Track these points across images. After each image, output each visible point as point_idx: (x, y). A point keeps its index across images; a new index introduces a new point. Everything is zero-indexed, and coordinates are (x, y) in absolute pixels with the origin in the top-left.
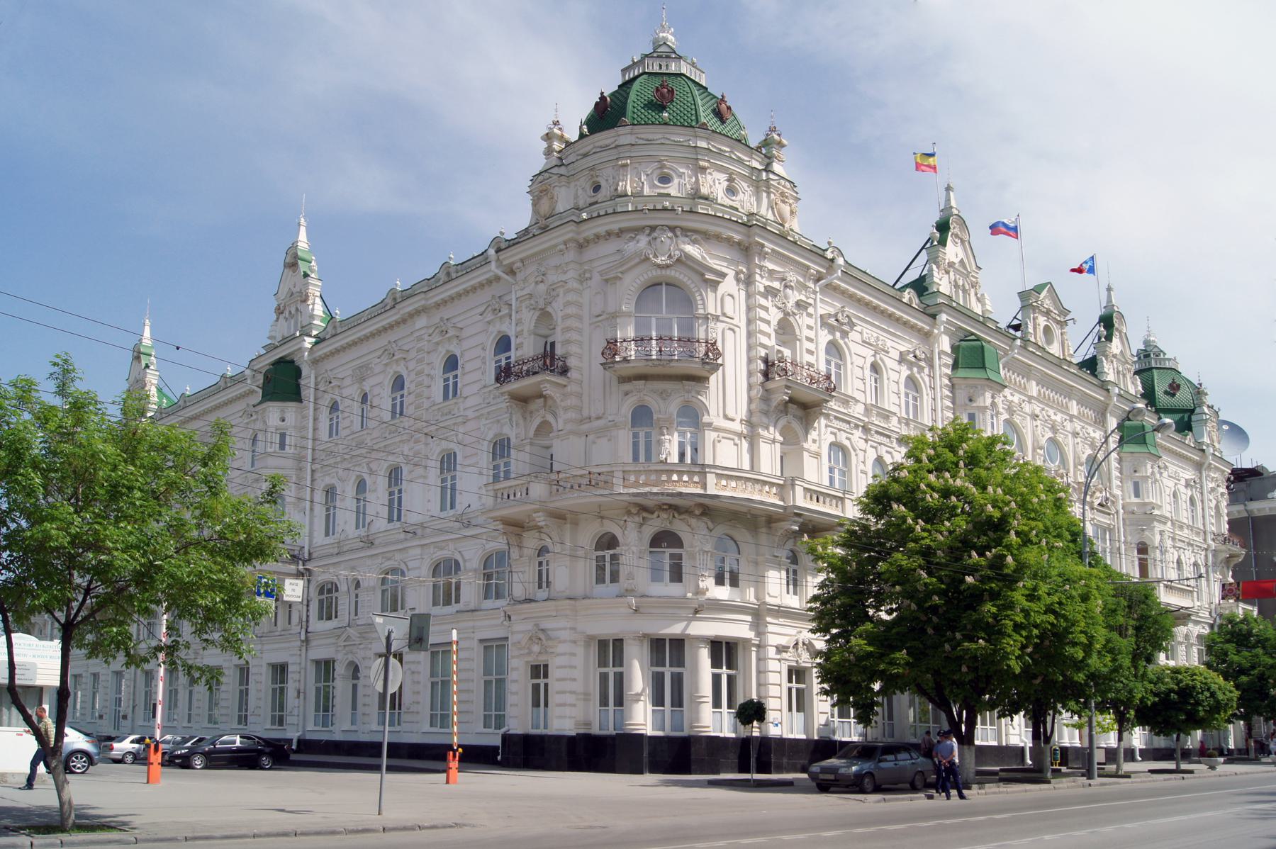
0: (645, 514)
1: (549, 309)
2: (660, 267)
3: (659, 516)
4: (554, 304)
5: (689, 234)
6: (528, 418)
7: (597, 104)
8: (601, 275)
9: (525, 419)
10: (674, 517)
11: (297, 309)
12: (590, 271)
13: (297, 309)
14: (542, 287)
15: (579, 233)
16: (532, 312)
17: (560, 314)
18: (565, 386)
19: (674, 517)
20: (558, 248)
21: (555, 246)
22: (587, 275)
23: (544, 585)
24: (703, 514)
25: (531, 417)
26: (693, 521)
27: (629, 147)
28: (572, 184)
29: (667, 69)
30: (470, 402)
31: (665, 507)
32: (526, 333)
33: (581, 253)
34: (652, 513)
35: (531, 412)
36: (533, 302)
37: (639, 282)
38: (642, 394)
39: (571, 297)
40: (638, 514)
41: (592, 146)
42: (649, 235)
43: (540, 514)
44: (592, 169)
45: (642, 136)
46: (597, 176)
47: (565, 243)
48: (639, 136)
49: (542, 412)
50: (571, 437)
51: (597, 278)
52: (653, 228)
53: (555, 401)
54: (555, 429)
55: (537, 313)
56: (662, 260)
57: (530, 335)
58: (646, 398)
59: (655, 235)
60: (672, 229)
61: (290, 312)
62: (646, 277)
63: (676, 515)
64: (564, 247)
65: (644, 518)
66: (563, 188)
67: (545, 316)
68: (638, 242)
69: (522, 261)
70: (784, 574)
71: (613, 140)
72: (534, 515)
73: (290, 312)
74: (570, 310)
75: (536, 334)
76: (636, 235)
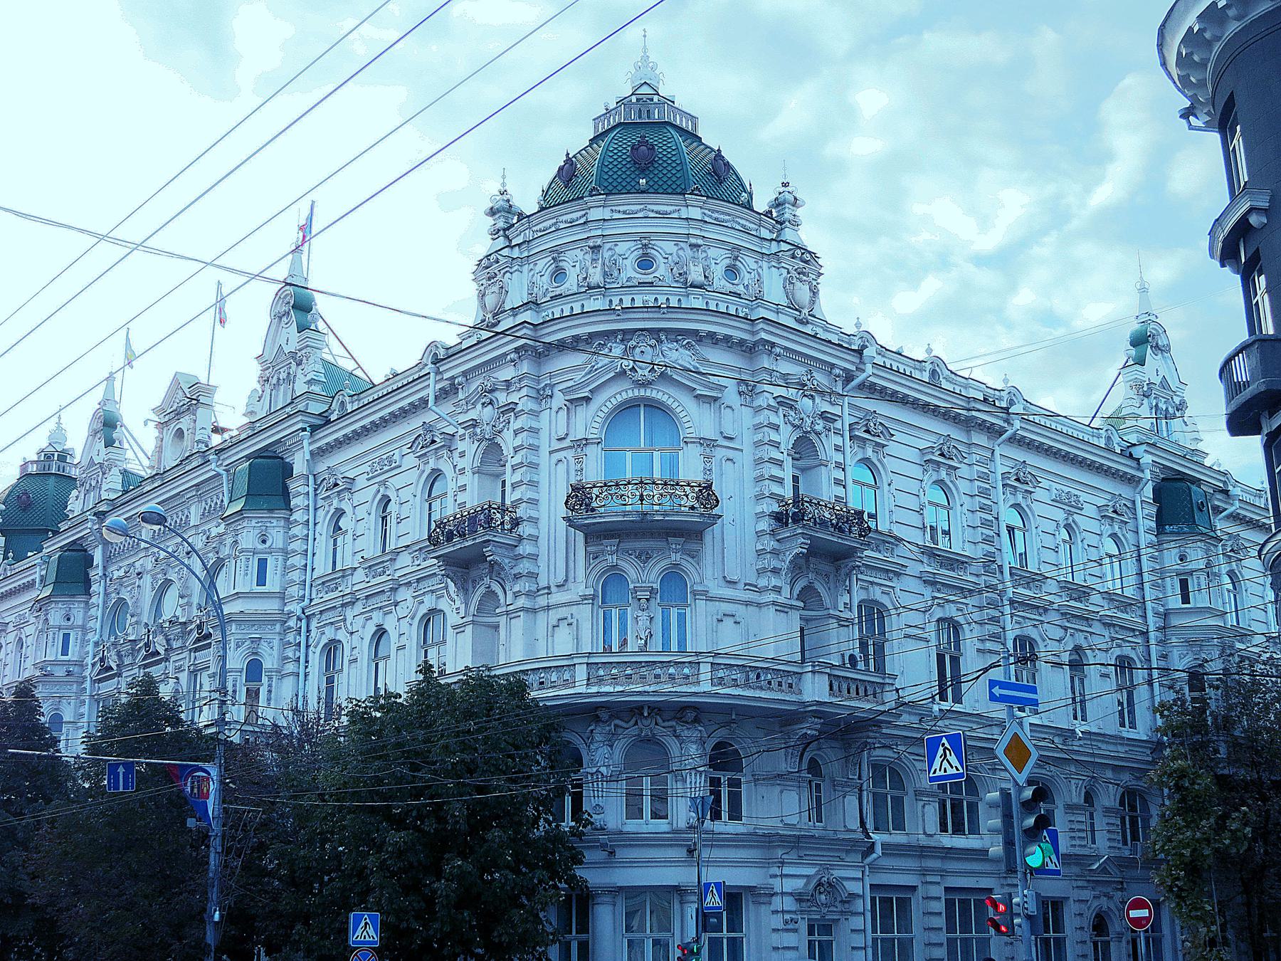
1: (499, 440)
5: (680, 338)
6: (471, 589)
7: (561, 169)
10: (656, 724)
12: (552, 386)
18: (516, 546)
21: (505, 355)
24: (697, 720)
25: (474, 588)
29: (649, 117)
33: (539, 364)
42: (622, 340)
47: (517, 350)
49: (487, 580)
50: (521, 613)
51: (559, 400)
53: (503, 569)
54: (502, 601)
59: (633, 343)
63: (660, 721)
64: (517, 355)
65: (616, 726)
67: (492, 450)
69: (464, 374)
70: (806, 794)
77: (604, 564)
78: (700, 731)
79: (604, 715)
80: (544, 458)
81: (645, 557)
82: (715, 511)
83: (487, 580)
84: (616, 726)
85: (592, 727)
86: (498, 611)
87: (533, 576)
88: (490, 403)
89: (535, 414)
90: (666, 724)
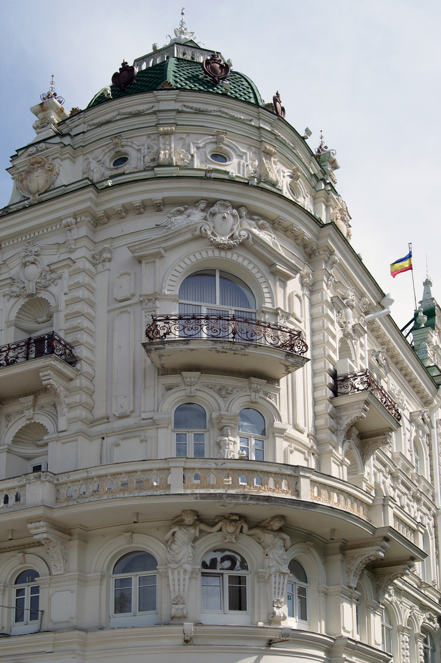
0: (203, 527)
2: (220, 247)
3: (220, 530)
4: (52, 288)
5: (256, 217)
8: (133, 252)
10: (241, 531)
14: (32, 270)
15: (97, 205)
17: (64, 298)
18: (71, 380)
19: (241, 531)
20: (64, 222)
21: (60, 220)
22: (106, 255)
27: (174, 113)
28: (80, 159)
31: (234, 517)
34: (213, 525)
35: (8, 416)
36: (14, 289)
37: (184, 266)
38: (193, 388)
39: (81, 278)
40: (193, 525)
41: (116, 113)
43: (42, 523)
44: (118, 135)
45: (191, 105)
46: (123, 146)
48: (186, 104)
52: (211, 203)
55: (22, 302)
56: (223, 239)
58: (199, 394)
60: (237, 207)
62: (199, 257)
64: (73, 221)
65: (201, 531)
66: (68, 161)
68: (189, 216)
71: (150, 105)
72: (29, 526)
74: (81, 293)
75: (17, 327)
76: (186, 209)
85: (174, 530)
88: (33, 263)
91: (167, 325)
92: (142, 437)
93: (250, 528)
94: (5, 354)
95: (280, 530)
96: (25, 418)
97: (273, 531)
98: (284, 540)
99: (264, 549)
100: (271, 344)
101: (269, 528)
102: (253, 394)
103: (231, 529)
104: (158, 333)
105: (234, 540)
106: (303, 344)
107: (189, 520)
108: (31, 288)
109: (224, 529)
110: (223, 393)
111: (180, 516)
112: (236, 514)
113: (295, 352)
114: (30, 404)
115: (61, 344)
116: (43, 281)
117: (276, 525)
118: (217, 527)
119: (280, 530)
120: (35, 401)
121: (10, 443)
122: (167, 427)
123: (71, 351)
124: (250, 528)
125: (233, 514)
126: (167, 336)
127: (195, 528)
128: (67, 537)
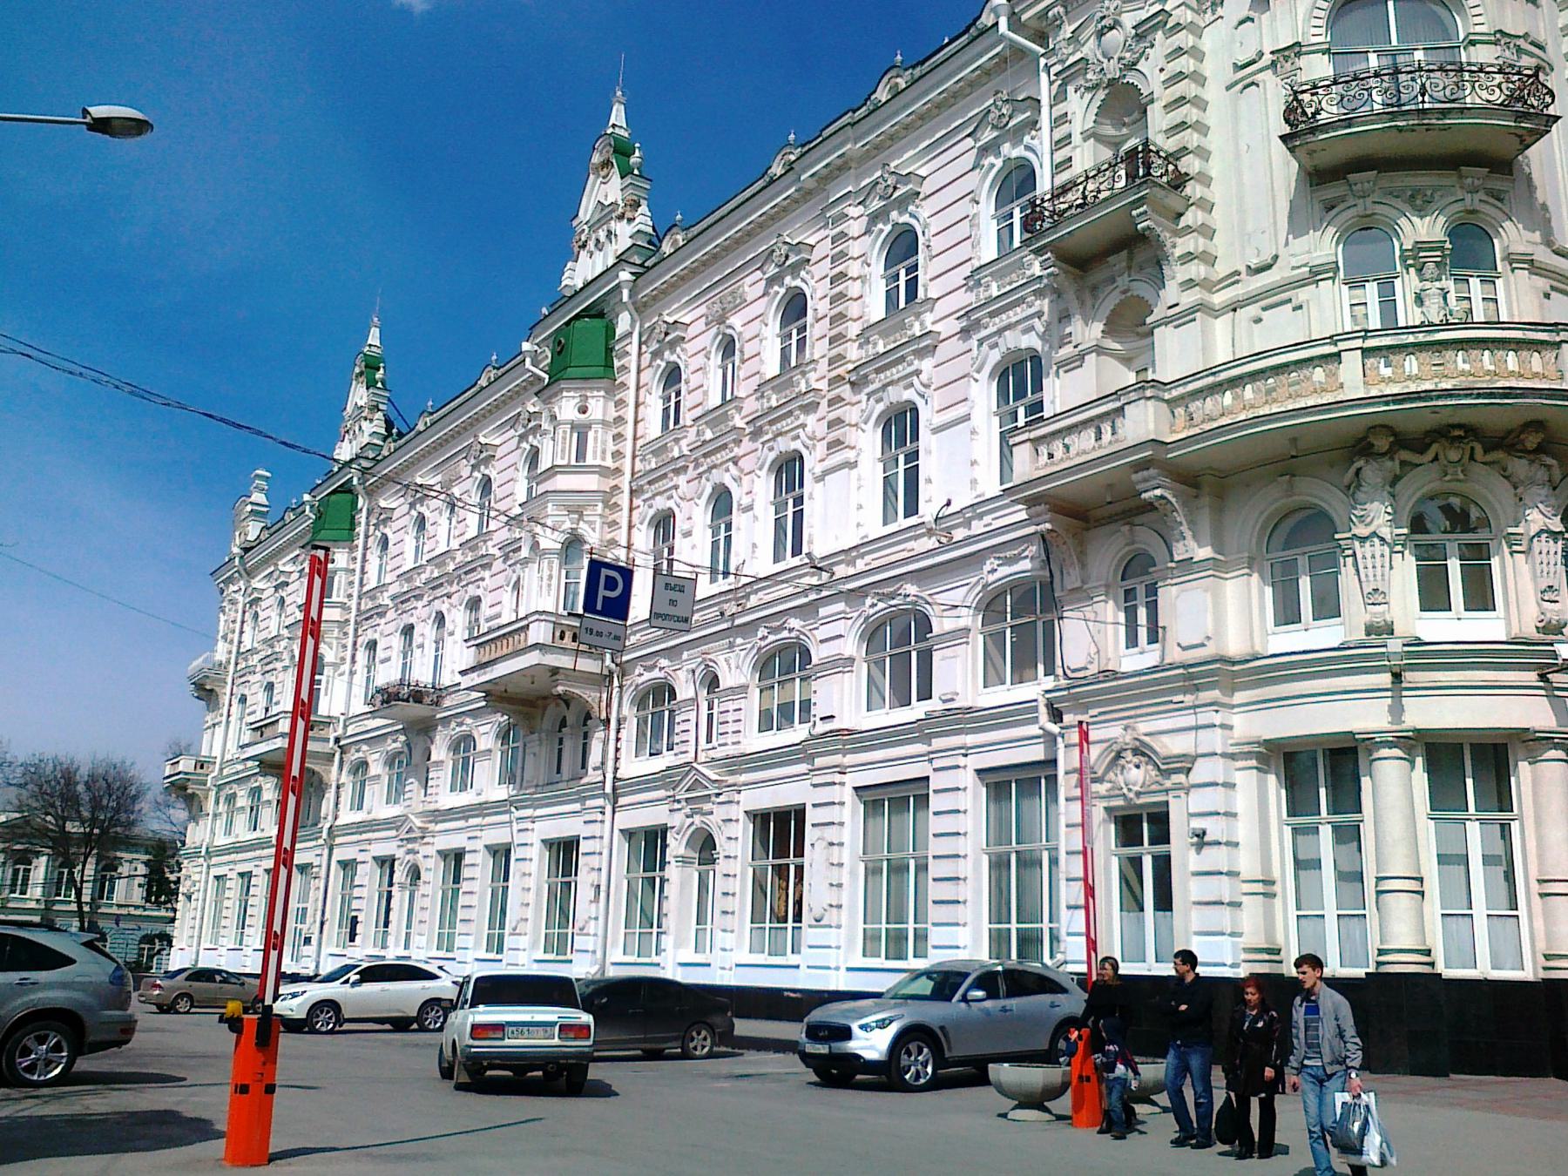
0: (1405, 455)
1: (1131, 78)
3: (1436, 459)
6: (1089, 303)
9: (1082, 303)
10: (1472, 458)
11: (610, 232)
13: (610, 232)
16: (1088, 96)
19: (1472, 458)
23: (1143, 633)
25: (1095, 297)
26: (1519, 467)
30: (942, 308)
31: (1457, 433)
32: (1077, 138)
38: (1369, 200)
39: (1184, 39)
40: (1390, 453)
43: (1152, 472)
57: (1085, 140)
58: (1379, 209)
61: (598, 241)
65: (1403, 463)
72: (1135, 477)
73: (598, 241)
74: (1185, 64)
77: (1353, 212)
78: (1549, 467)
79: (1382, 443)
80: (1213, 92)
81: (1420, 204)
82: (1551, 111)
83: (1122, 281)
84: (1403, 463)
86: (1149, 320)
87: (1209, 259)
89: (1197, 31)
90: (1489, 458)
91: (1315, 98)
92: (1295, 303)
93: (1486, 452)
94: (1081, 187)
95: (1540, 449)
96: (1118, 290)
97: (1529, 452)
98: (1549, 467)
99: (1516, 488)
100: (1488, 101)
101: (1519, 447)
102: (1468, 197)
103: (1454, 455)
104: (1304, 113)
105: (1461, 476)
106: (1545, 91)
107: (1382, 443)
108: (1113, 69)
109: (1441, 457)
110: (1418, 202)
111: (1365, 438)
112: (1460, 426)
113: (1533, 106)
114: (1124, 264)
115: (1160, 157)
116: (1128, 55)
117: (1532, 441)
118: (1430, 455)
119: (1540, 449)
120: (1130, 258)
121: (1100, 335)
122: (1333, 279)
123: (1176, 166)
124: (1486, 452)
125: (1454, 426)
126: (1318, 117)
127: (1392, 459)
128: (1193, 491)
